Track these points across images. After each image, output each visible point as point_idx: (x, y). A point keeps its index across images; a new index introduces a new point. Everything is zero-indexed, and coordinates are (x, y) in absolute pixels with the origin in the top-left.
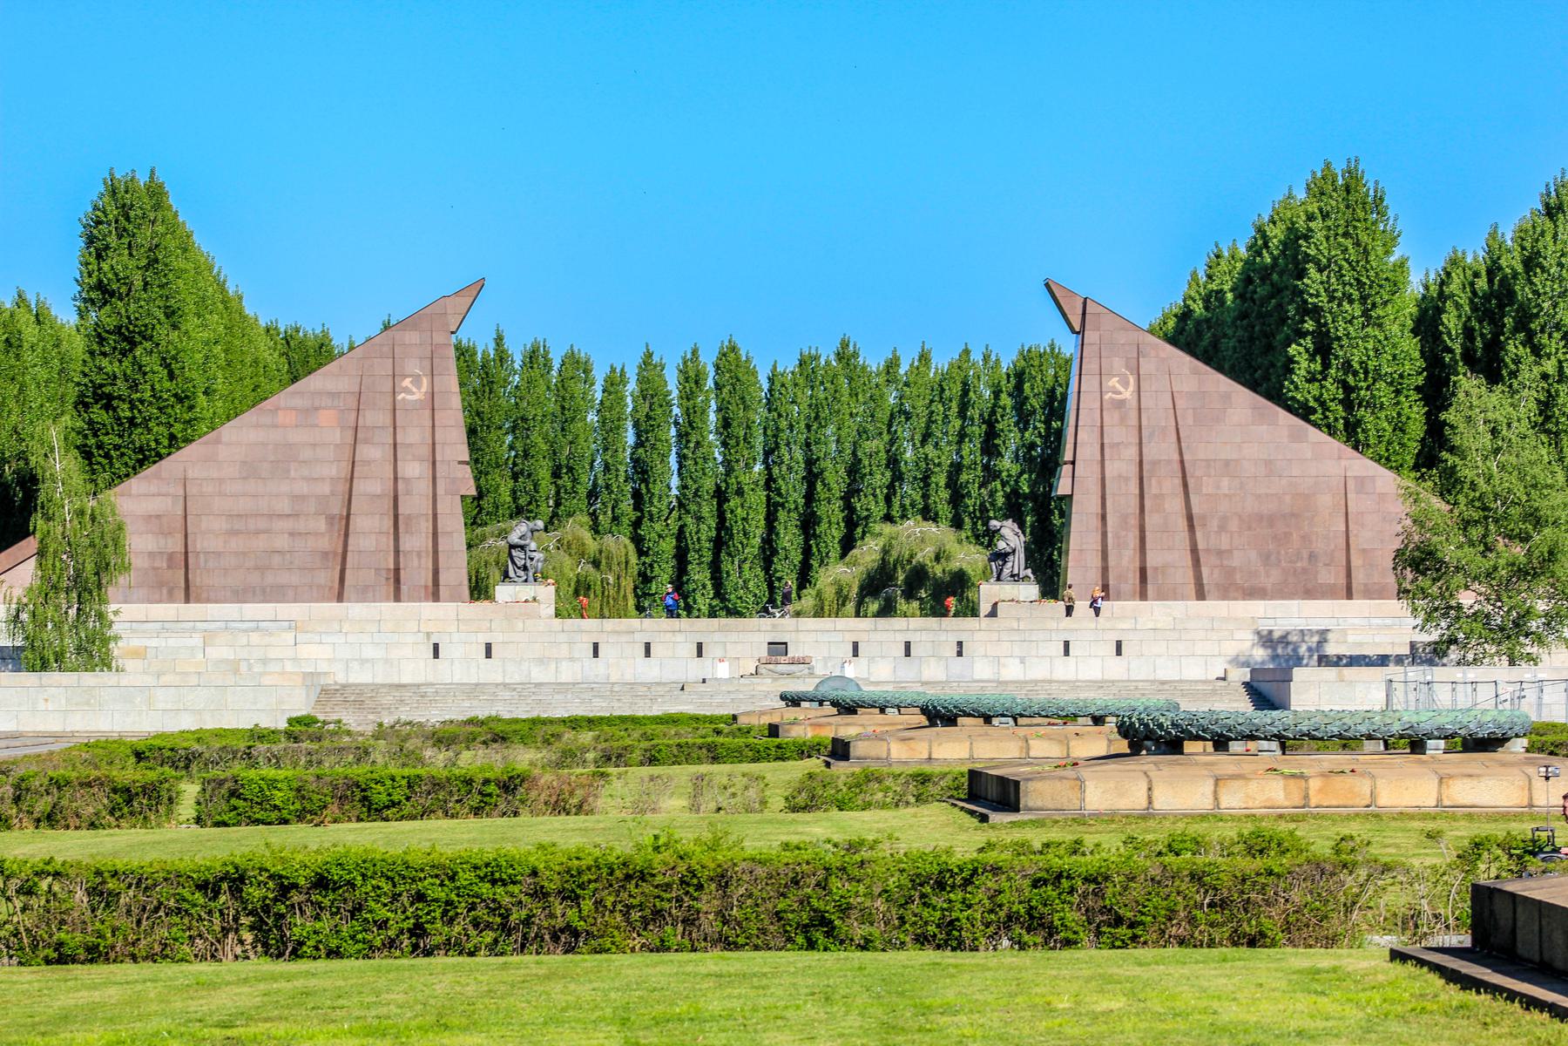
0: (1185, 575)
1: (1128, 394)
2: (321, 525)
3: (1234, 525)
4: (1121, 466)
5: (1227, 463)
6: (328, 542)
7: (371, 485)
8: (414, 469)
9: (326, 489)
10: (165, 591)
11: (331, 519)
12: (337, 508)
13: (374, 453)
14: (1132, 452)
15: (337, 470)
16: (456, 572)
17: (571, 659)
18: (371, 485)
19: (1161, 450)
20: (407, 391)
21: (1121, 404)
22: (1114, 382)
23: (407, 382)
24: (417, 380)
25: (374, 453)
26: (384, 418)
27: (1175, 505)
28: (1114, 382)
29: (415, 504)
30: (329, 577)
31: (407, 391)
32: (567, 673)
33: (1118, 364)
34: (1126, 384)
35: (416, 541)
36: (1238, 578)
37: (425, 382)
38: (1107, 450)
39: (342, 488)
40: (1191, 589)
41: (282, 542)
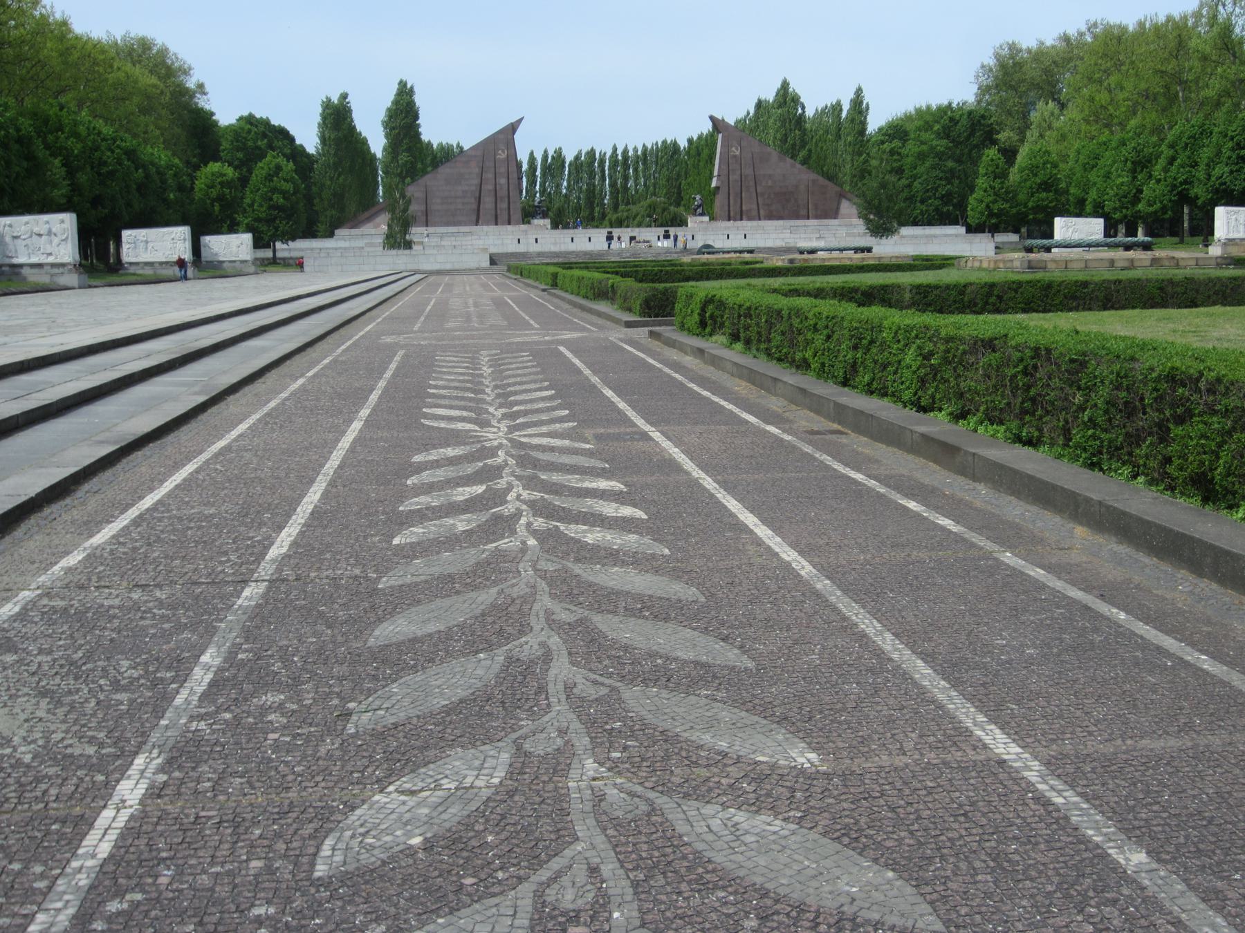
0: (755, 213)
1: (738, 153)
2: (473, 200)
4: (735, 177)
6: (475, 206)
8: (503, 181)
9: (473, 188)
15: (476, 181)
16: (516, 214)
19: (748, 171)
21: (735, 156)
25: (490, 176)
26: (492, 164)
27: (753, 190)
29: (502, 193)
32: (563, 248)
33: (735, 143)
41: (460, 206)
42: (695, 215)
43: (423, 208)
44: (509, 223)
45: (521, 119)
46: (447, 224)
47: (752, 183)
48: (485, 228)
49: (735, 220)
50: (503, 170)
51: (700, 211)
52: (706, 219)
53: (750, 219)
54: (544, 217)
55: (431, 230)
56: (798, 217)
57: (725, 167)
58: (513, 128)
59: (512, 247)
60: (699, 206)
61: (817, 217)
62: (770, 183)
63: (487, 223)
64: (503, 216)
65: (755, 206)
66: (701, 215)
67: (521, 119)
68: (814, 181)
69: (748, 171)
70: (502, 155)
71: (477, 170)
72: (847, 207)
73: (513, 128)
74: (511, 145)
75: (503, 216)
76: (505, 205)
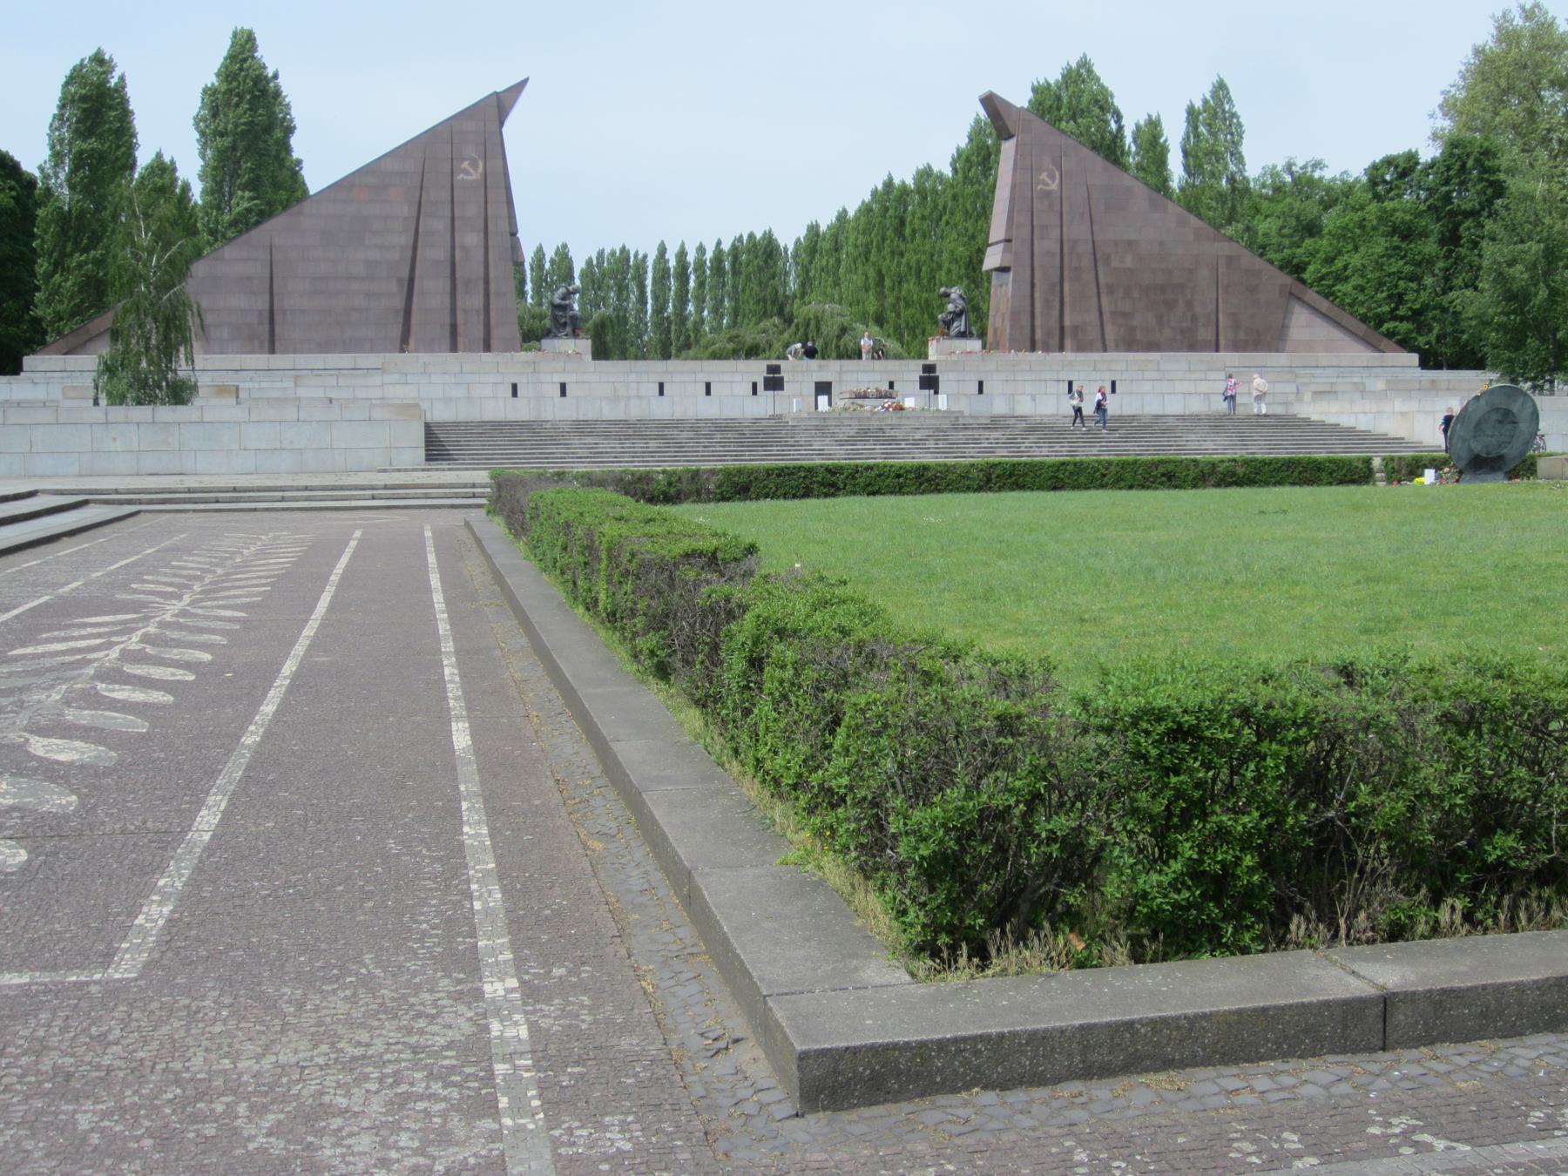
0: (1094, 333)
1: (1054, 186)
2: (393, 287)
3: (1135, 295)
4: (1046, 245)
5: (1130, 243)
6: (399, 303)
7: (434, 253)
8: (471, 239)
10: (256, 343)
11: (400, 280)
12: (405, 274)
13: (436, 224)
14: (1056, 233)
15: (405, 240)
16: (507, 328)
17: (639, 397)
18: (434, 253)
20: (466, 172)
21: (1048, 194)
22: (1044, 176)
23: (465, 165)
24: (474, 164)
25: (436, 224)
27: (1089, 276)
28: (1044, 176)
29: (470, 269)
30: (396, 331)
31: (466, 172)
32: (635, 412)
34: (1053, 178)
35: (471, 301)
36: (1139, 336)
37: (481, 164)
38: (1036, 232)
39: (409, 254)
40: (1099, 345)
42: (946, 335)
43: (262, 303)
44: (487, 347)
45: (519, 87)
46: (326, 346)
47: (1087, 261)
48: (424, 357)
49: (1047, 349)
50: (472, 211)
51: (959, 325)
52: (975, 345)
53: (1081, 347)
54: (575, 335)
55: (280, 360)
56: (1193, 347)
57: (1023, 219)
58: (499, 106)
59: (498, 408)
60: (958, 315)
61: (1237, 346)
62: (1129, 261)
63: (430, 347)
64: (472, 328)
65: (1093, 317)
66: (962, 335)
67: (519, 87)
68: (1230, 260)
69: (1078, 231)
70: (470, 174)
71: (405, 210)
72: (1303, 323)
73: (499, 106)
74: (493, 150)
75: (472, 328)
76: (477, 301)
